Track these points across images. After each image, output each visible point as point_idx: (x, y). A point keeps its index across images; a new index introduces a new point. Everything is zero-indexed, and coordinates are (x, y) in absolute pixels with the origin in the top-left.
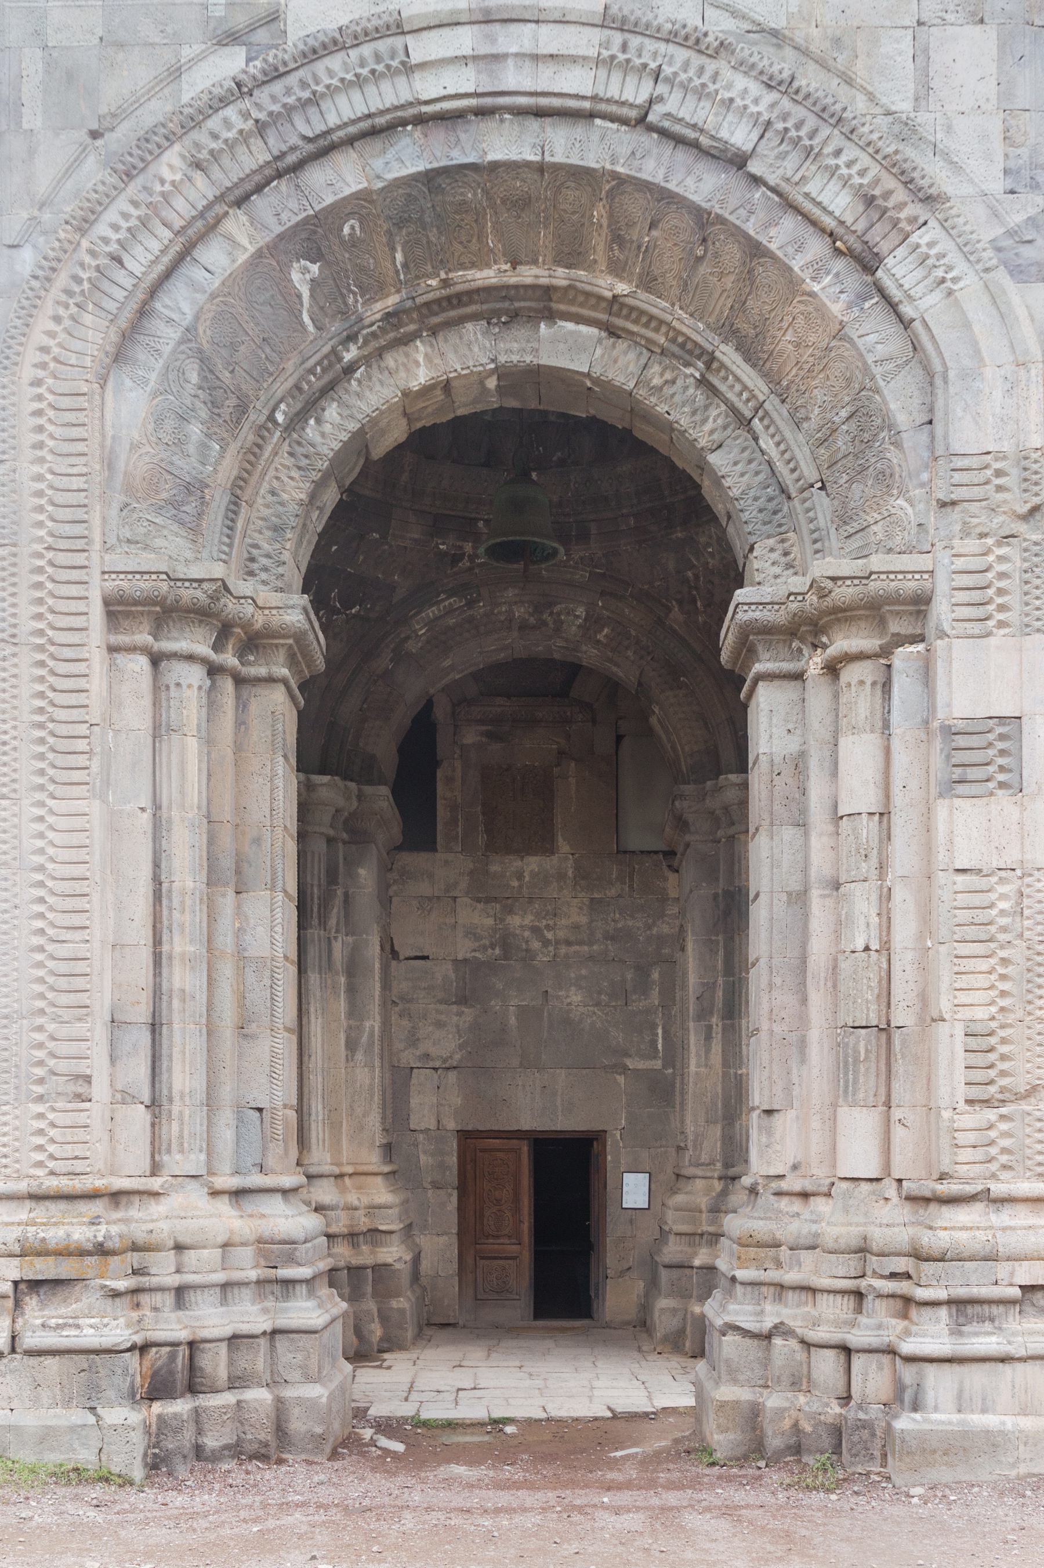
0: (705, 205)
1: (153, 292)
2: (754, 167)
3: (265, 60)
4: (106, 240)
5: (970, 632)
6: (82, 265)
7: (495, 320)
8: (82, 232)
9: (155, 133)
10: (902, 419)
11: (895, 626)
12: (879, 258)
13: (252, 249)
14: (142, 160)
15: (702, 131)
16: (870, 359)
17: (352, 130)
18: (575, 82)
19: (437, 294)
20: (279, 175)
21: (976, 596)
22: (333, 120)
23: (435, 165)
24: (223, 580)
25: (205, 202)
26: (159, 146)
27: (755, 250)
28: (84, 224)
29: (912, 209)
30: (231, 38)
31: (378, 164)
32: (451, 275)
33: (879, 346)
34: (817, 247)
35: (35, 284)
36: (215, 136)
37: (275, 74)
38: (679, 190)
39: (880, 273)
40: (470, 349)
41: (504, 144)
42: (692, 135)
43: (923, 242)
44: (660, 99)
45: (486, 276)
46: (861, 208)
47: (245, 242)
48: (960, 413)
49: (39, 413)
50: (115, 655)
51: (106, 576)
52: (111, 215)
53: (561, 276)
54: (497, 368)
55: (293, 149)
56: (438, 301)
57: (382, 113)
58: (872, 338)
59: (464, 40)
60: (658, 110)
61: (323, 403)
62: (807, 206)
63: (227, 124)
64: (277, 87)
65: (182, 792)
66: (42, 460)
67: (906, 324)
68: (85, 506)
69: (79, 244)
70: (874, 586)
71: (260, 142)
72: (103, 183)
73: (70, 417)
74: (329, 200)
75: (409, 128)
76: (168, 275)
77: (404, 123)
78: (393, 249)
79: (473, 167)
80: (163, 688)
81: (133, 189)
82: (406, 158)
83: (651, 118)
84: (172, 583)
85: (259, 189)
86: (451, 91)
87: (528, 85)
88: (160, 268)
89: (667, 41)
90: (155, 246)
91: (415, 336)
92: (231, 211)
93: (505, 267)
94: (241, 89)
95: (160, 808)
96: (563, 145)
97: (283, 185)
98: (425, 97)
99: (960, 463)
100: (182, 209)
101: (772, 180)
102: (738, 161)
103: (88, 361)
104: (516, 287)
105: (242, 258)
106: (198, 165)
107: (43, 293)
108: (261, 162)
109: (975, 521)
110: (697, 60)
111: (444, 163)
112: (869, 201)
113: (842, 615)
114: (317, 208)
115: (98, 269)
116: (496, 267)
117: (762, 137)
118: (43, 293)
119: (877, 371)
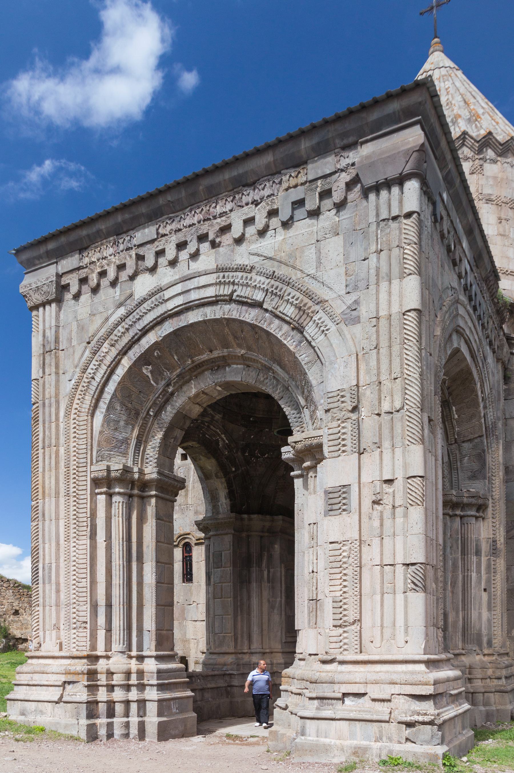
0: (252, 322)
2: (265, 306)
4: (90, 374)
5: (334, 456)
8: (84, 373)
12: (303, 328)
15: (248, 298)
21: (336, 442)
22: (146, 322)
28: (84, 371)
31: (159, 333)
34: (286, 327)
35: (73, 390)
38: (244, 319)
41: (193, 317)
42: (245, 300)
43: (316, 319)
44: (235, 291)
46: (297, 311)
48: (330, 377)
52: (91, 366)
55: (136, 334)
57: (158, 317)
58: (304, 356)
60: (235, 294)
61: (166, 406)
62: (281, 315)
74: (147, 347)
83: (234, 297)
85: (130, 348)
86: (176, 305)
87: (197, 297)
98: (169, 309)
100: (109, 359)
101: (270, 309)
105: (126, 370)
106: (112, 345)
109: (335, 415)
111: (178, 327)
112: (300, 309)
115: (88, 382)
117: (266, 295)
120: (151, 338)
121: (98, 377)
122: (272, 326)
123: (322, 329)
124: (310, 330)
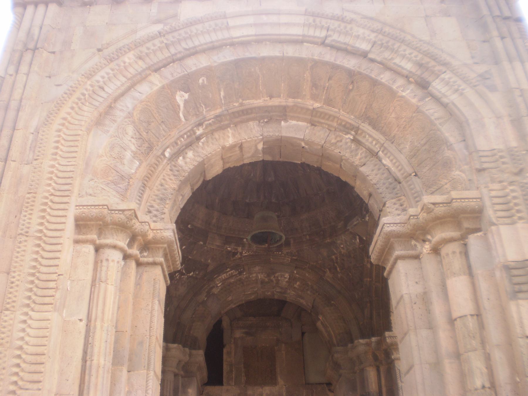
1: (116, 100)
3: (171, 26)
4: (98, 82)
6: (86, 90)
7: (262, 121)
8: (89, 78)
9: (124, 48)
10: (452, 140)
11: (466, 225)
13: (160, 85)
14: (117, 56)
16: (433, 118)
17: (205, 46)
18: (297, 31)
19: (238, 109)
20: (174, 62)
22: (197, 43)
23: (239, 57)
24: (134, 210)
25: (141, 69)
26: (125, 51)
27: (375, 83)
28: (89, 75)
29: (437, 68)
30: (158, 21)
32: (244, 102)
33: (436, 114)
34: (401, 82)
36: (148, 49)
37: (173, 30)
38: (341, 64)
39: (430, 88)
40: (251, 131)
44: (330, 36)
45: (259, 102)
47: (157, 83)
49: (57, 142)
50: (77, 245)
51: (77, 208)
52: (102, 73)
53: (291, 102)
54: (263, 138)
55: (180, 52)
56: (238, 112)
59: (251, 20)
63: (154, 45)
64: (176, 34)
65: (103, 313)
66: (55, 159)
67: (445, 106)
68: (72, 177)
69: (86, 83)
70: (455, 204)
71: (167, 50)
72: (100, 63)
73: (72, 144)
74: (194, 69)
75: (228, 47)
76: (123, 94)
77: (226, 45)
78: (220, 91)
79: (254, 59)
80: (99, 262)
81: (113, 65)
82: (227, 56)
83: (327, 41)
84: (109, 212)
85: (165, 66)
88: (120, 91)
89: (331, 19)
90: (119, 83)
91: (228, 126)
92: (152, 74)
93: (266, 99)
94: (160, 34)
95: (90, 321)
96: (290, 51)
97: (175, 65)
99: (481, 154)
101: (379, 59)
102: (364, 55)
103: (83, 123)
104: (272, 107)
105: (155, 88)
106: (140, 58)
107: (67, 99)
108: (167, 56)
110: (343, 25)
112: (420, 65)
113: (440, 221)
114: (189, 71)
116: (262, 99)
118: (67, 99)
119: (437, 122)
120: (202, 62)
121: (112, 89)
122: (382, 76)
123: (456, 87)
124: (437, 86)
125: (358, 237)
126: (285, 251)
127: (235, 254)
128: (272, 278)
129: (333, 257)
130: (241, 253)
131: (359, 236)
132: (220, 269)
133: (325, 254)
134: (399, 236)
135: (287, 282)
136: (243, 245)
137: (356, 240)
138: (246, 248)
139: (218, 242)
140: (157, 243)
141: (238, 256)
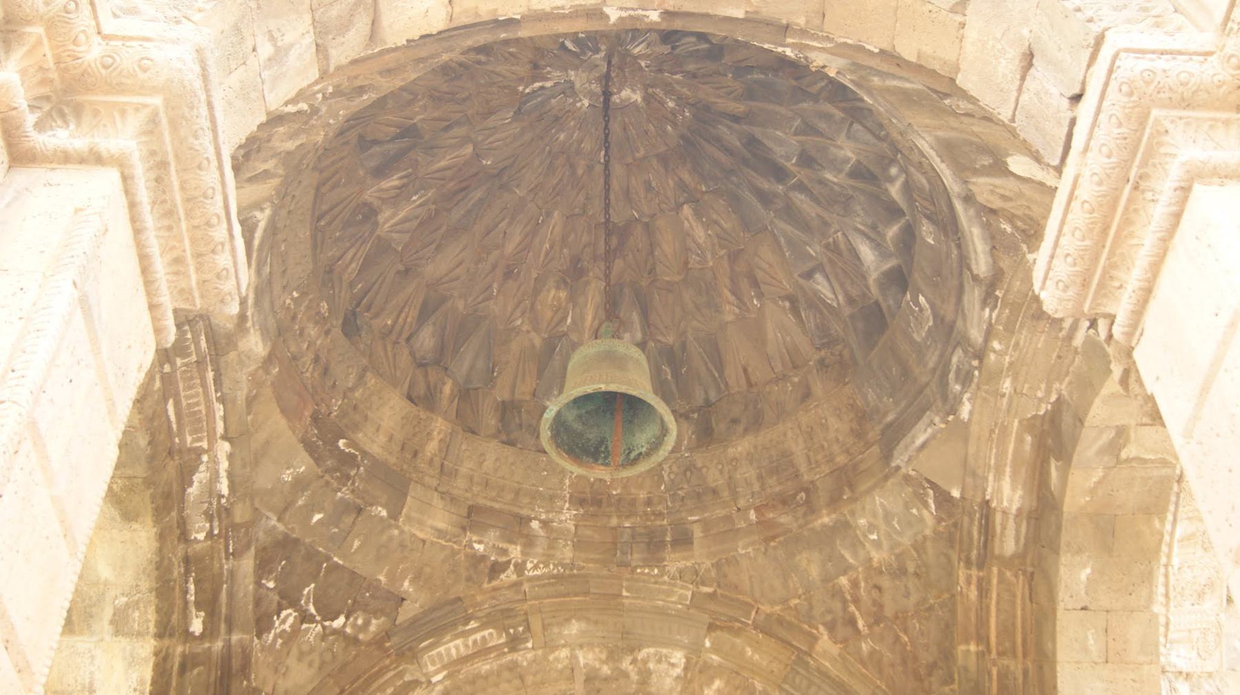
125: (931, 492)
126: (675, 562)
127: (496, 569)
128: (626, 664)
129: (843, 581)
130: (520, 568)
131: (933, 486)
132: (443, 618)
133: (815, 572)
134: (1187, 100)
135: (678, 677)
136: (529, 542)
137: (926, 505)
138: (539, 550)
139: (441, 519)
140: (120, 89)
141: (509, 576)
